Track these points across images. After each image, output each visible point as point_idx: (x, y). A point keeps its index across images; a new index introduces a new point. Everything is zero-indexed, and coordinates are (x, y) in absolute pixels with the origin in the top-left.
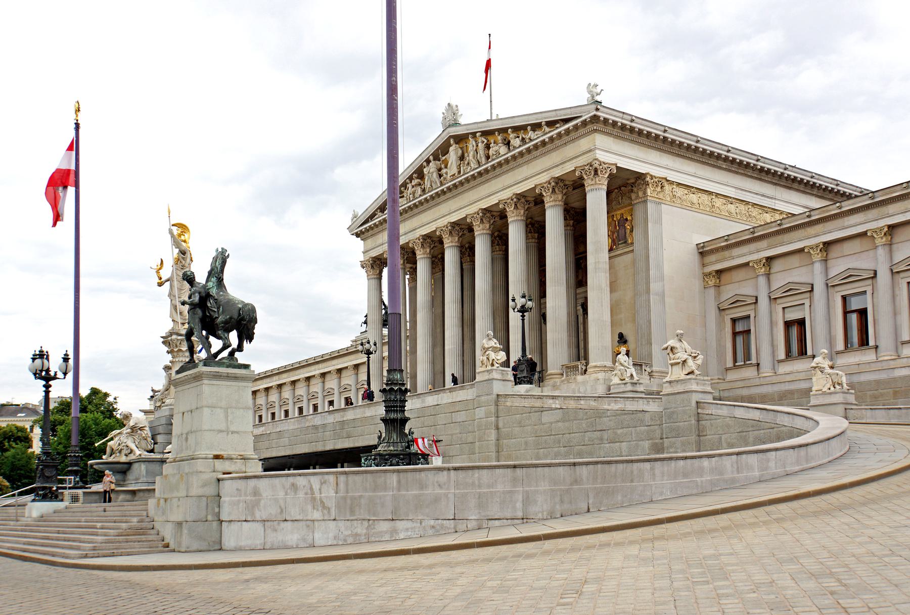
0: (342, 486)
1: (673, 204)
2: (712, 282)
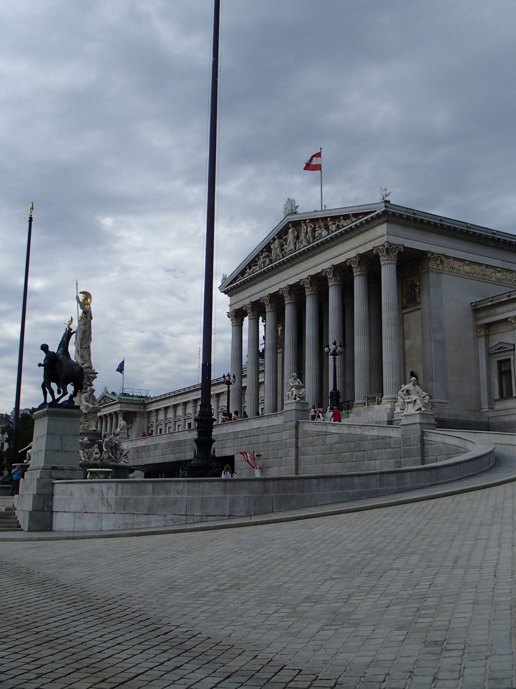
0: (119, 490)
1: (450, 273)
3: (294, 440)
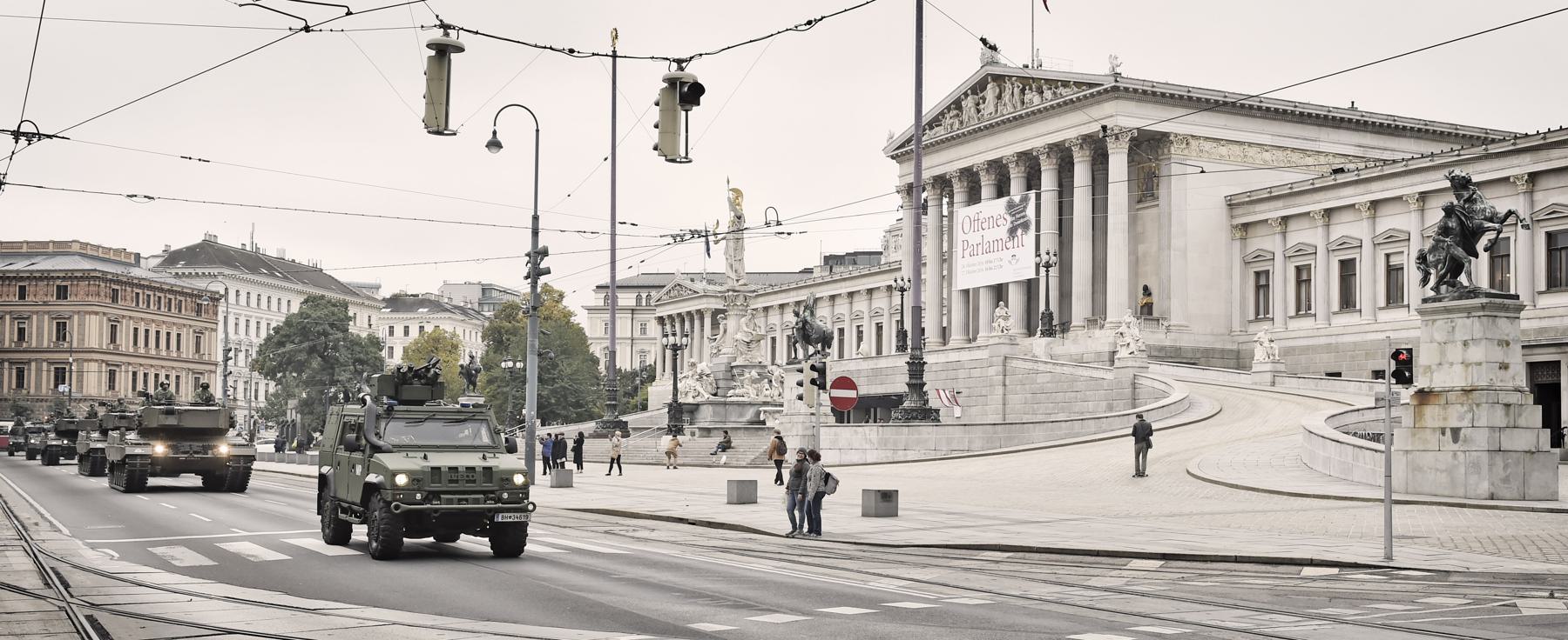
0: (880, 432)
2: (1238, 235)
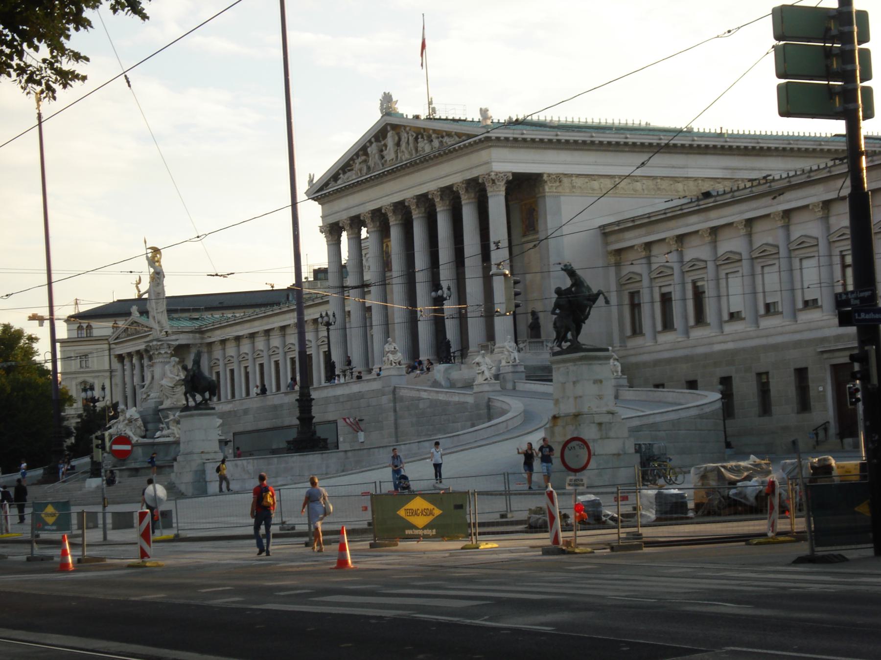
2: (612, 260)
3: (392, 405)
